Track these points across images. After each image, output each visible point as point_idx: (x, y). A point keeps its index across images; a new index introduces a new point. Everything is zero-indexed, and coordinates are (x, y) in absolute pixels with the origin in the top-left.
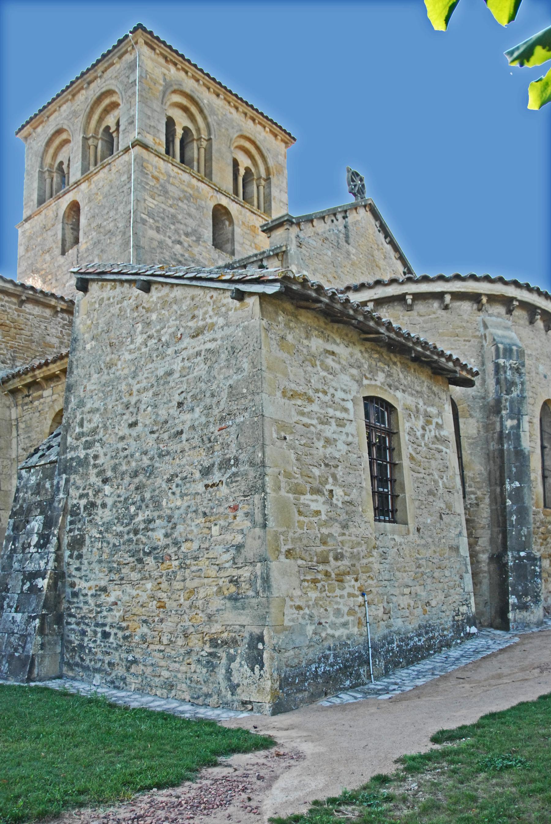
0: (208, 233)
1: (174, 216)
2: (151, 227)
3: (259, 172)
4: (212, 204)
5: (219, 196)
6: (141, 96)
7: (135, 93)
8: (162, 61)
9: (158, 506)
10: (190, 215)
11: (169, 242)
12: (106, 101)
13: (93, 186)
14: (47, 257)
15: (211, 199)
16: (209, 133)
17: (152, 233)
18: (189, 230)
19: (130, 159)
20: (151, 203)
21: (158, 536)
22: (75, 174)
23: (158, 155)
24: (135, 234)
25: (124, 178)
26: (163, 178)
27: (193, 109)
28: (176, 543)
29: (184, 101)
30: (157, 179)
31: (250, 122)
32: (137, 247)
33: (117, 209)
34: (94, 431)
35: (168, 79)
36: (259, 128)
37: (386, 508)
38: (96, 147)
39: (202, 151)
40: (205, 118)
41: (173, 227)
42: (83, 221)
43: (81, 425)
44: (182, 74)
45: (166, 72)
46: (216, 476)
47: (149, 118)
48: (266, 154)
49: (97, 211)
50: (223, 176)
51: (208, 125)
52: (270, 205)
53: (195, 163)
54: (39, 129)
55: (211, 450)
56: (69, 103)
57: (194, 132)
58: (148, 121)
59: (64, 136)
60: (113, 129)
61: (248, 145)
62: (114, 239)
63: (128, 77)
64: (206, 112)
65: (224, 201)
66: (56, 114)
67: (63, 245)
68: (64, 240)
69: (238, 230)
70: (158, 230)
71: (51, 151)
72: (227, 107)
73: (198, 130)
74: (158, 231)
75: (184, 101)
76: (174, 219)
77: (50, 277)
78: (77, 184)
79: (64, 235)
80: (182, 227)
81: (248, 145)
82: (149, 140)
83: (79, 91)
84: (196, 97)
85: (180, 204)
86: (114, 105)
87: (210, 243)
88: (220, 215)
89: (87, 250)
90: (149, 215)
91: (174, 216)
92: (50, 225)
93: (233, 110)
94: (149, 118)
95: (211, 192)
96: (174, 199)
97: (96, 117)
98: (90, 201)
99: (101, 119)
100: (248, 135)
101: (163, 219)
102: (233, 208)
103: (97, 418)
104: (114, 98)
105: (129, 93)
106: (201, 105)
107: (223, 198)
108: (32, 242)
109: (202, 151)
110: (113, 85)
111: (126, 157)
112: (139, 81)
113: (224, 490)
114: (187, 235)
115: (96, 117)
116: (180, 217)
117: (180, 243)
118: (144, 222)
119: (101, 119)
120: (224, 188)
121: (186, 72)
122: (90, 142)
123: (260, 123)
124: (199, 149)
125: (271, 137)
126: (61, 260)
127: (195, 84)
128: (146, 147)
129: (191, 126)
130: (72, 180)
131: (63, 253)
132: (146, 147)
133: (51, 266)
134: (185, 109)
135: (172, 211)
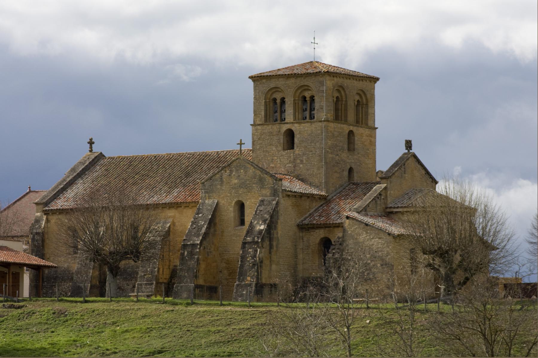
0: (346, 146)
9: (371, 270)
12: (306, 88)
15: (346, 129)
16: (346, 99)
21: (371, 276)
25: (319, 132)
28: (375, 278)
31: (361, 82)
34: (352, 253)
40: (345, 92)
43: (348, 250)
46: (384, 266)
51: (346, 94)
52: (367, 117)
55: (383, 261)
63: (320, 87)
65: (351, 128)
69: (356, 138)
73: (341, 96)
93: (355, 81)
98: (300, 133)
103: (353, 250)
104: (309, 88)
109: (343, 106)
110: (310, 84)
112: (326, 93)
113: (386, 269)
115: (299, 91)
117: (338, 155)
118: (328, 151)
119: (301, 92)
124: (341, 105)
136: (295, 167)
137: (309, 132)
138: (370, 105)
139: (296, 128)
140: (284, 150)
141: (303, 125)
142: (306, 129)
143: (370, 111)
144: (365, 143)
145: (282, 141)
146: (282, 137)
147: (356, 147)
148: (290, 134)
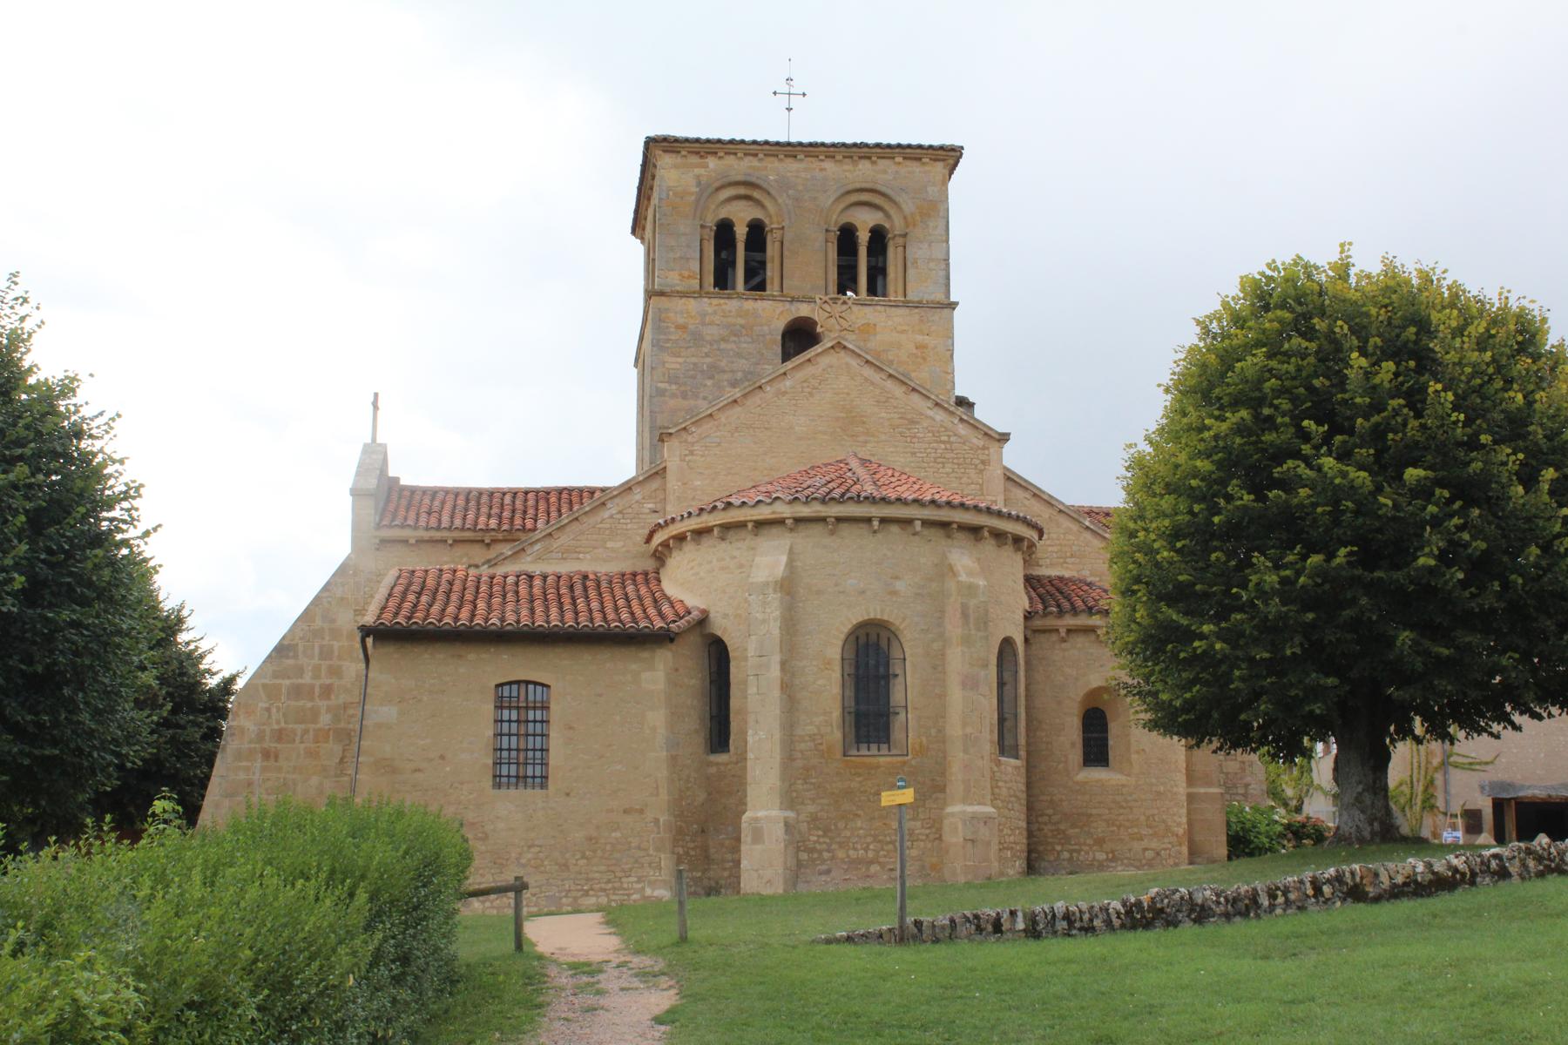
2: (674, 396)
8: (694, 159)
20: (673, 363)
27: (756, 194)
29: (742, 191)
30: (683, 327)
35: (704, 180)
41: (709, 383)
45: (702, 171)
48: (897, 199)
57: (767, 221)
58: (671, 255)
61: (865, 197)
64: (773, 192)
70: (684, 396)
75: (742, 191)
84: (753, 179)
85: (723, 345)
91: (713, 367)
95: (780, 307)
100: (858, 186)
101: (694, 377)
106: (765, 186)
116: (723, 364)
127: (755, 162)
134: (747, 198)
135: (708, 360)
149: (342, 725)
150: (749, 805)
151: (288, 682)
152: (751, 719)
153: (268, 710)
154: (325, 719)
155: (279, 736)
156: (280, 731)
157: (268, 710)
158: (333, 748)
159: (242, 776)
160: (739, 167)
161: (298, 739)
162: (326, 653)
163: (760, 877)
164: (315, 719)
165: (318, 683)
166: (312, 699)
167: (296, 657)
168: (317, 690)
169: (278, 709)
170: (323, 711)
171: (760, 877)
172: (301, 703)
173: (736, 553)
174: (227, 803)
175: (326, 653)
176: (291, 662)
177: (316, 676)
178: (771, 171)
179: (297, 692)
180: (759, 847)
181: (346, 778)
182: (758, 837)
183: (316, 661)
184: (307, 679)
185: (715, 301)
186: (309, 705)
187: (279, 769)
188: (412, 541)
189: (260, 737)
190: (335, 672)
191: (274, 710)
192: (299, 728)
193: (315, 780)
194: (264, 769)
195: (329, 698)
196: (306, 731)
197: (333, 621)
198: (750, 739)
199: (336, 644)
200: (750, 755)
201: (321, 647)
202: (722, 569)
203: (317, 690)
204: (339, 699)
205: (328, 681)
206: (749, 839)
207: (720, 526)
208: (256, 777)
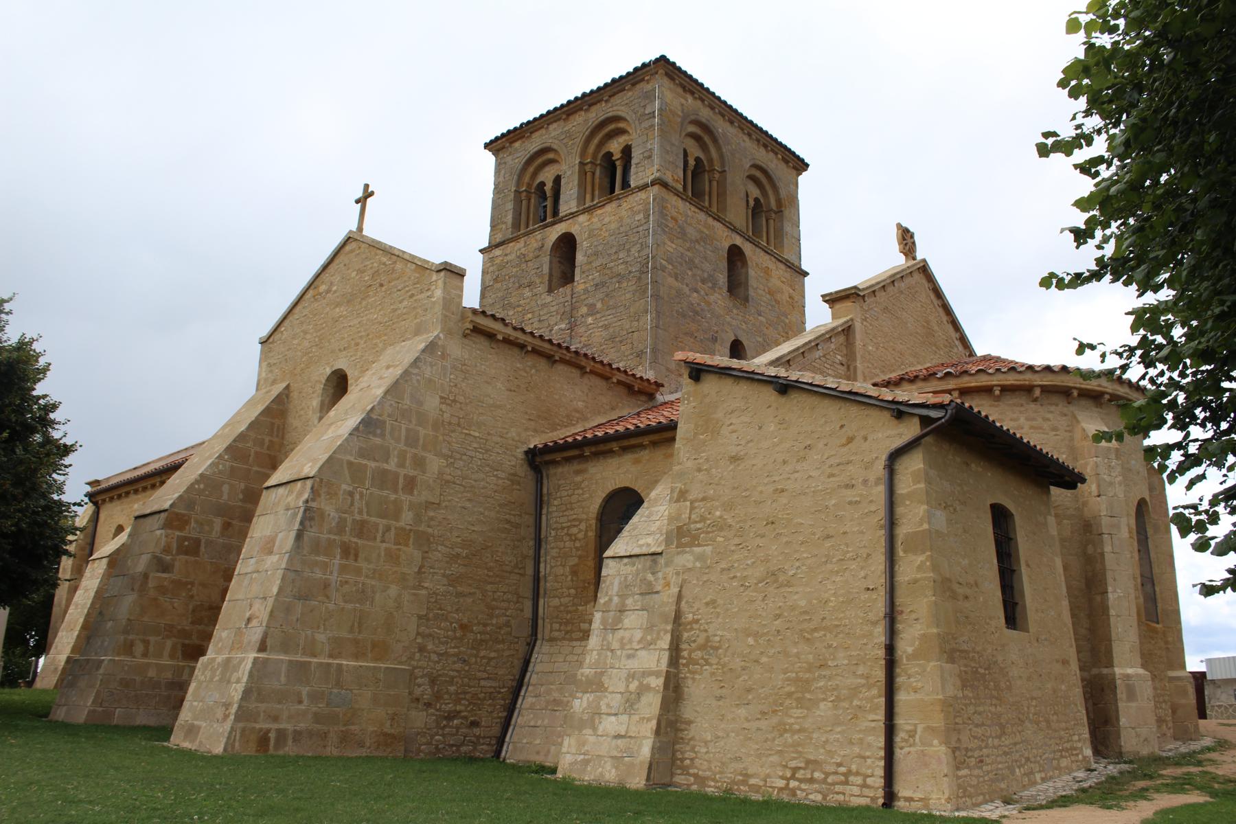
0: (722, 279)
1: (691, 261)
2: (670, 275)
3: (769, 203)
4: (726, 245)
5: (735, 236)
6: (661, 130)
7: (653, 126)
8: (680, 90)
10: (705, 258)
11: (686, 290)
12: (612, 126)
13: (595, 220)
14: (527, 293)
15: (726, 239)
16: (723, 165)
17: (671, 280)
18: (706, 275)
19: (648, 198)
20: (670, 247)
22: (568, 203)
23: (677, 194)
24: (655, 282)
26: (681, 219)
27: (707, 139)
30: (676, 221)
31: (762, 150)
32: (656, 296)
33: (629, 251)
36: (771, 154)
37: (1013, 615)
38: (594, 174)
39: (715, 183)
40: (719, 148)
42: (580, 258)
44: (699, 102)
45: (683, 101)
47: (668, 152)
49: (600, 248)
50: (738, 213)
51: (722, 156)
53: (707, 198)
54: (517, 144)
56: (561, 123)
59: (551, 156)
60: (617, 156)
62: (625, 284)
63: (645, 106)
64: (720, 141)
65: (738, 241)
66: (543, 131)
67: (550, 281)
68: (551, 275)
69: (752, 273)
71: (531, 169)
72: (741, 135)
73: (711, 160)
74: (676, 279)
76: (691, 264)
77: (530, 316)
78: (573, 215)
79: (551, 269)
80: (699, 272)
81: (758, 174)
82: (668, 178)
83: (575, 112)
86: (622, 132)
87: (725, 289)
88: (735, 255)
89: (586, 291)
90: (669, 261)
91: (691, 261)
92: (531, 255)
93: (746, 138)
94: (668, 152)
96: (691, 241)
97: (596, 141)
99: (602, 144)
102: (747, 248)
104: (622, 125)
105: (646, 124)
107: (738, 237)
108: (504, 272)
109: (715, 183)
110: (622, 111)
111: (642, 195)
114: (703, 281)
115: (596, 141)
117: (697, 291)
118: (663, 269)
119: (602, 144)
120: (738, 225)
121: (703, 101)
122: (588, 168)
123: (772, 151)
124: (710, 182)
125: (783, 166)
126: (549, 299)
127: (711, 113)
128: (664, 185)
129: (702, 156)
130: (564, 209)
131: (550, 291)
132: (664, 185)
133: (533, 303)
136: (571, 329)
137: (613, 226)
138: (786, 213)
139: (578, 227)
140: (550, 291)
141: (599, 212)
142: (607, 220)
143: (788, 227)
144: (778, 297)
145: (546, 269)
146: (547, 259)
147: (751, 292)
148: (567, 245)
149: (422, 528)
150: (1116, 661)
151: (372, 464)
152: (1109, 575)
153: (351, 494)
154: (407, 517)
155: (361, 529)
156: (363, 523)
157: (351, 494)
158: (411, 552)
159: (318, 574)
160: (705, 114)
161: (379, 539)
162: (412, 440)
163: (1138, 735)
164: (397, 517)
165: (402, 472)
166: (396, 492)
167: (383, 436)
168: (401, 480)
169: (361, 495)
170: (406, 507)
171: (1138, 735)
172: (385, 493)
173: (1050, 416)
174: (299, 607)
175: (412, 440)
176: (378, 441)
177: (401, 465)
178: (721, 126)
179: (383, 479)
180: (1133, 704)
181: (424, 592)
182: (1131, 695)
183: (402, 446)
184: (392, 465)
185: (693, 208)
186: (393, 497)
187: (358, 571)
188: (500, 337)
189: (340, 528)
190: (420, 463)
191: (357, 496)
192: (382, 522)
193: (393, 590)
194: (343, 569)
195: (411, 493)
196: (388, 529)
197: (420, 403)
198: (1110, 595)
199: (422, 432)
200: (1112, 612)
201: (408, 430)
202: (1032, 427)
203: (401, 480)
204: (422, 496)
205: (412, 473)
206: (1124, 696)
207: (1041, 386)
208: (334, 578)
